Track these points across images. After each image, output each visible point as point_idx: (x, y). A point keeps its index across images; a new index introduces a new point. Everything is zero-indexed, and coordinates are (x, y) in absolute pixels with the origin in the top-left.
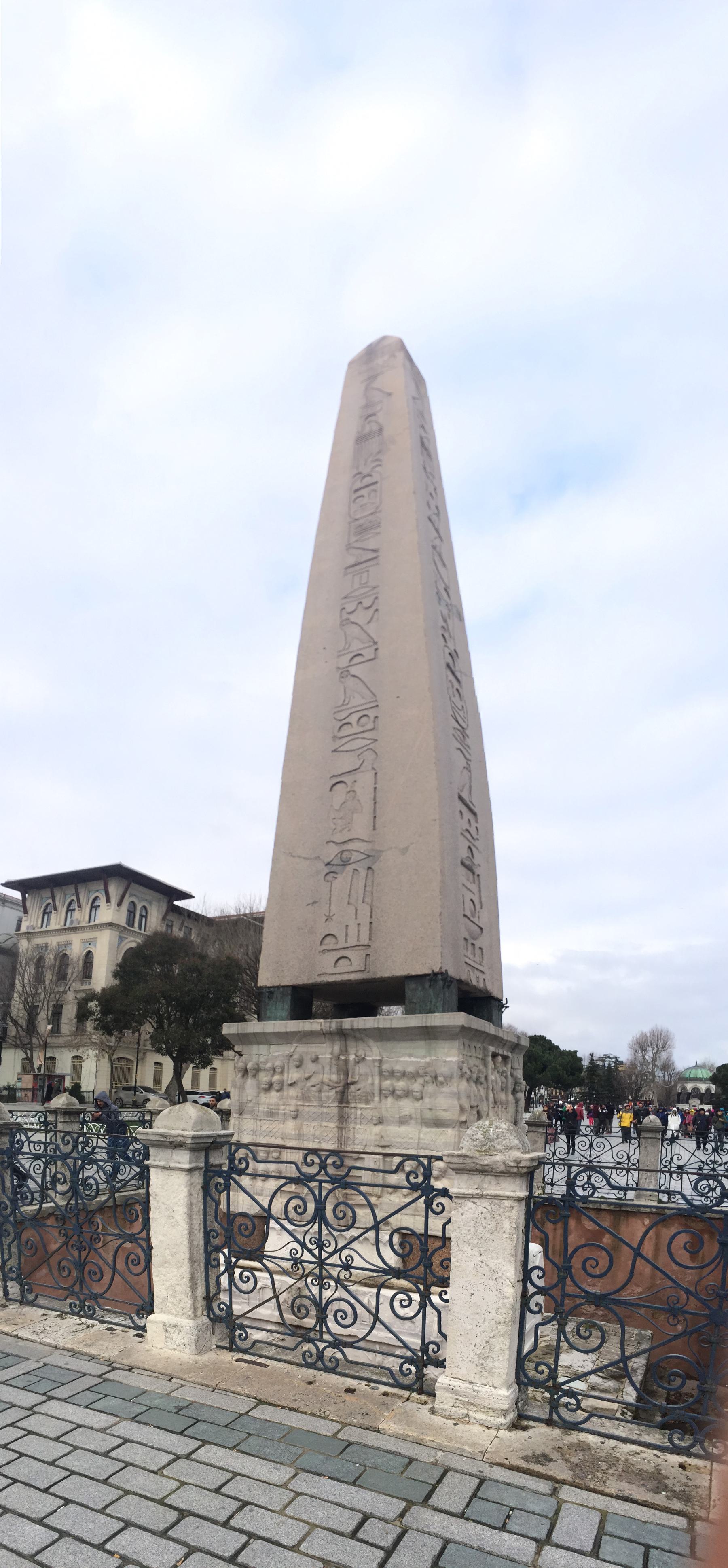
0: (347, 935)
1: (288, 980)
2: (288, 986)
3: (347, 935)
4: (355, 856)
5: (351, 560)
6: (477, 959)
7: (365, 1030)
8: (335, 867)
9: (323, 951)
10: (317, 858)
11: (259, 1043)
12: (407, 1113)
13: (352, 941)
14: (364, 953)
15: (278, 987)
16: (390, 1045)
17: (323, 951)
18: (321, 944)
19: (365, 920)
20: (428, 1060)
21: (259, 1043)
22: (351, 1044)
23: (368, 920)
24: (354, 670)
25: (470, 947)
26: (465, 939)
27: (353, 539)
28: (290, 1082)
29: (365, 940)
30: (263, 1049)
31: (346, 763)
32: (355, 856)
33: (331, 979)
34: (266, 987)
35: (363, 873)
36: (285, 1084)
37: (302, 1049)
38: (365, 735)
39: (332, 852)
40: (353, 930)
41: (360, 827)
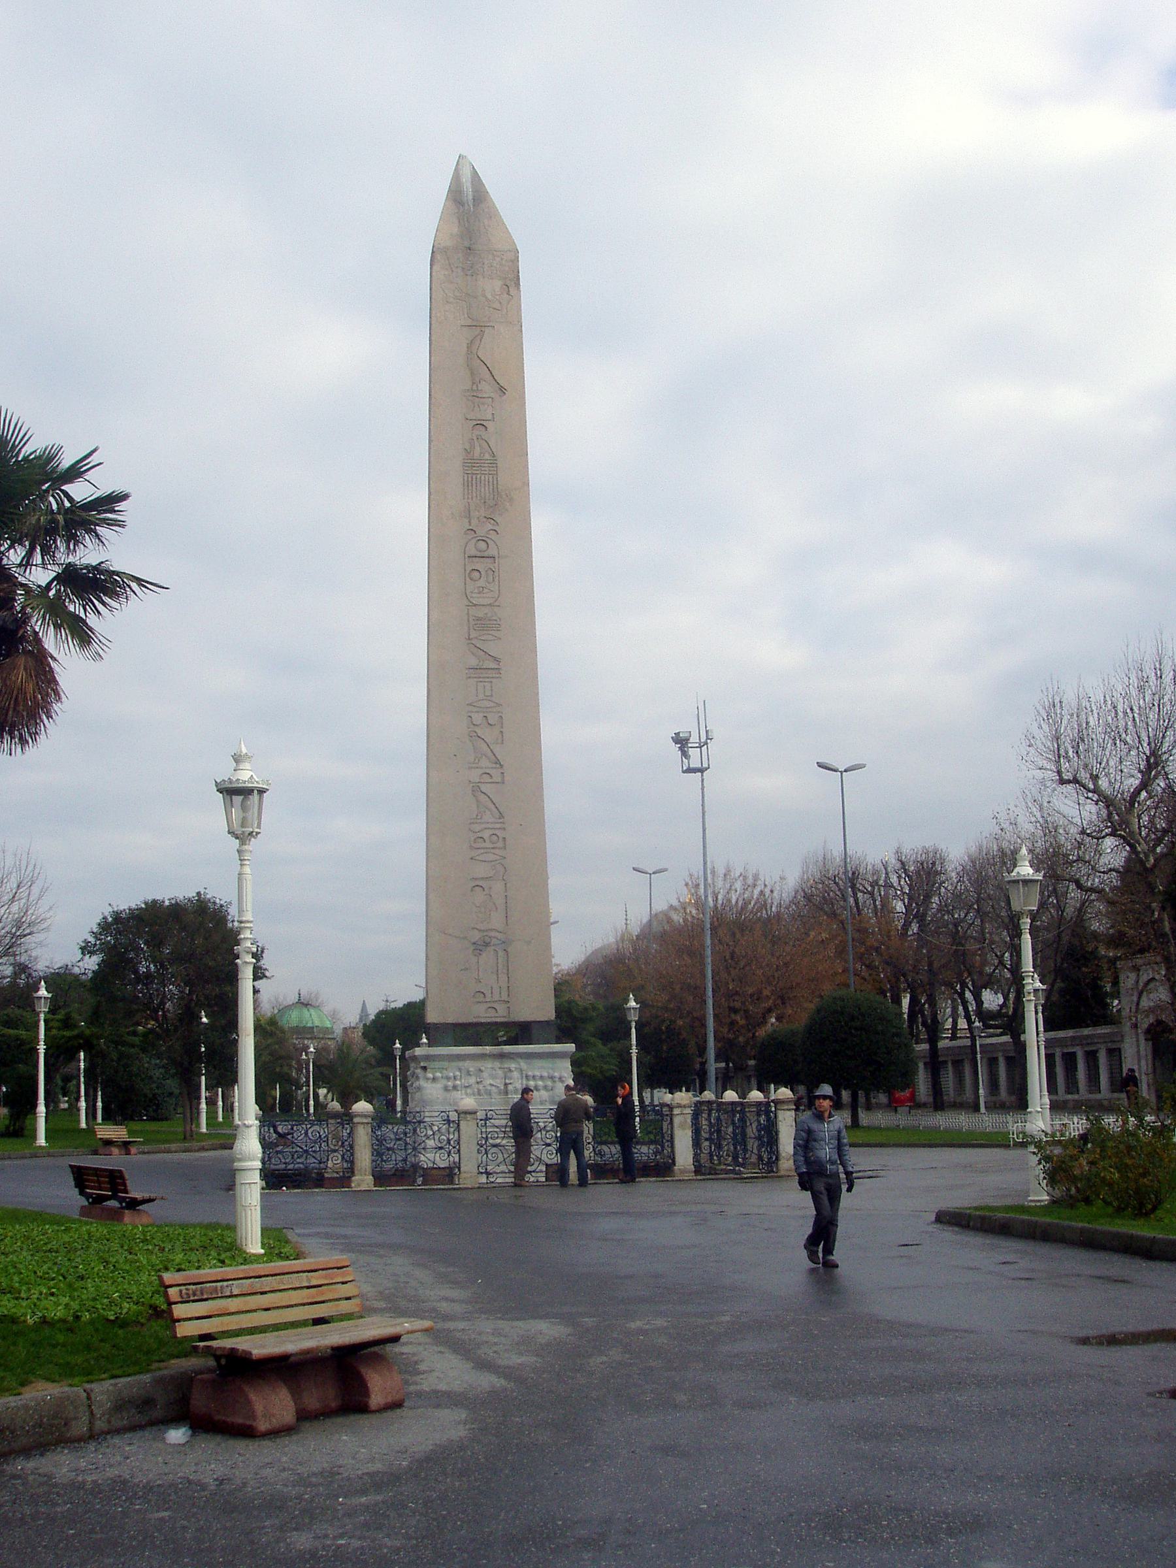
4: (494, 941)
5: (473, 662)
8: (481, 946)
10: (465, 938)
13: (496, 998)
19: (505, 985)
23: (506, 985)
24: (484, 788)
27: (473, 634)
29: (505, 997)
31: (481, 870)
32: (494, 941)
35: (501, 953)
38: (497, 851)
39: (476, 936)
40: (496, 991)
41: (497, 921)
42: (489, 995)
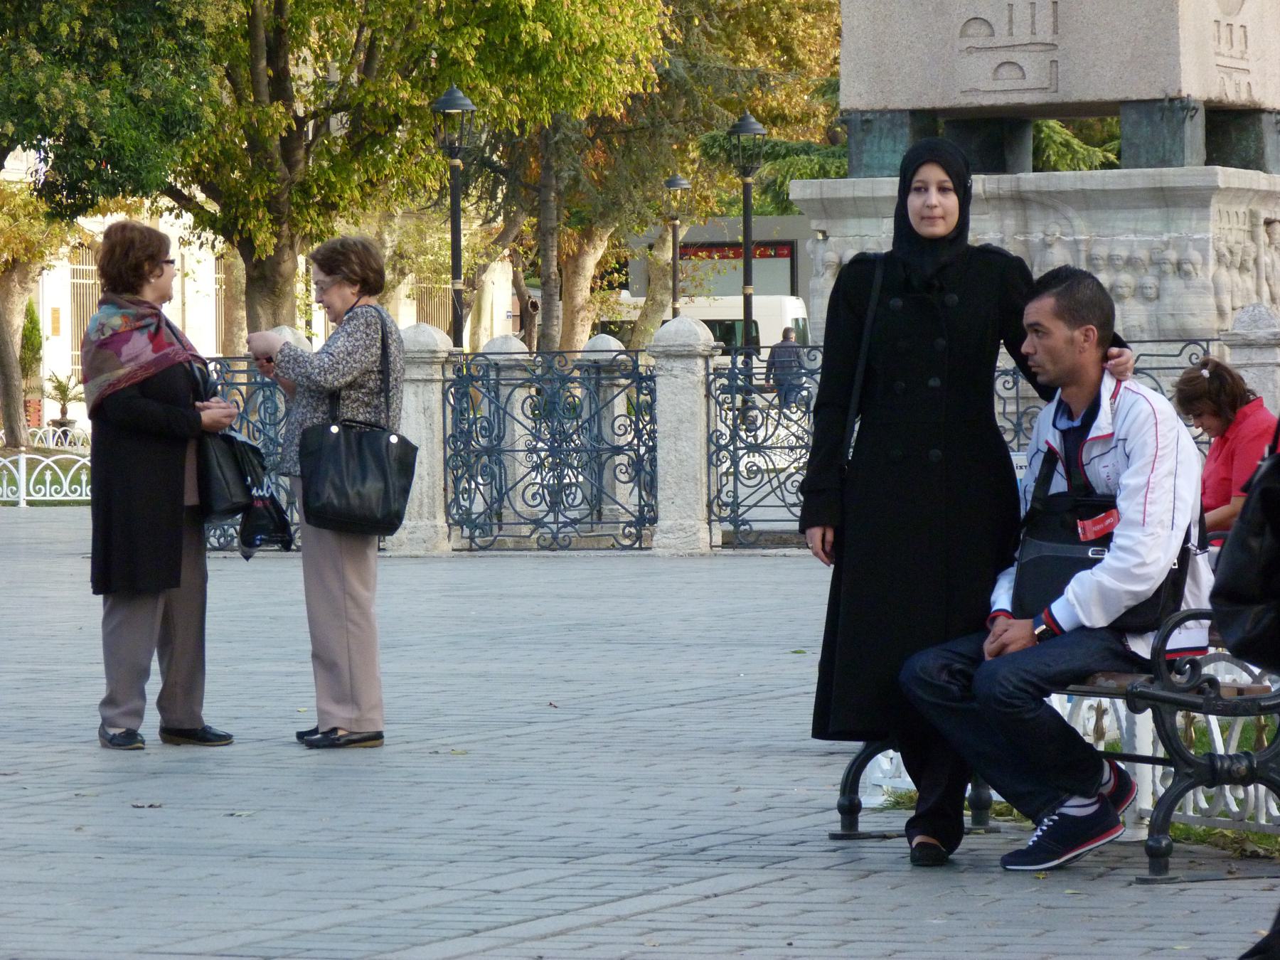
0: (1011, 21)
1: (903, 99)
2: (901, 111)
3: (1011, 21)
6: (1238, 47)
7: (1061, 193)
9: (970, 50)
11: (860, 215)
12: (1136, 323)
13: (1022, 35)
14: (1045, 58)
15: (882, 112)
16: (1099, 215)
17: (970, 50)
18: (963, 34)
20: (1165, 238)
22: (1035, 212)
25: (1224, 32)
26: (1217, 21)
33: (987, 101)
34: (857, 111)
40: (1022, 14)
42: (1001, 27)
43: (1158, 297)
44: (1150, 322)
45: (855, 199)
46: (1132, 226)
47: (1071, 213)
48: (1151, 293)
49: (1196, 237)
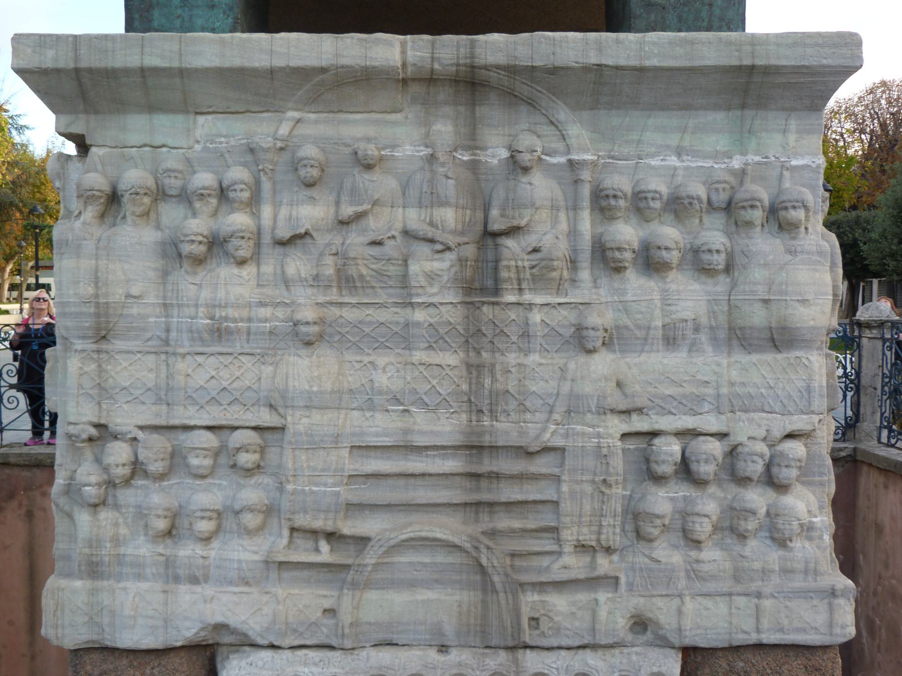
7: (554, 71)
12: (688, 315)
16: (616, 119)
21: (152, 108)
22: (491, 111)
28: (284, 233)
30: (167, 128)
36: (267, 239)
37: (311, 131)
43: (728, 269)
44: (712, 314)
45: (143, 72)
46: (674, 140)
47: (562, 114)
48: (719, 260)
49: (794, 163)
